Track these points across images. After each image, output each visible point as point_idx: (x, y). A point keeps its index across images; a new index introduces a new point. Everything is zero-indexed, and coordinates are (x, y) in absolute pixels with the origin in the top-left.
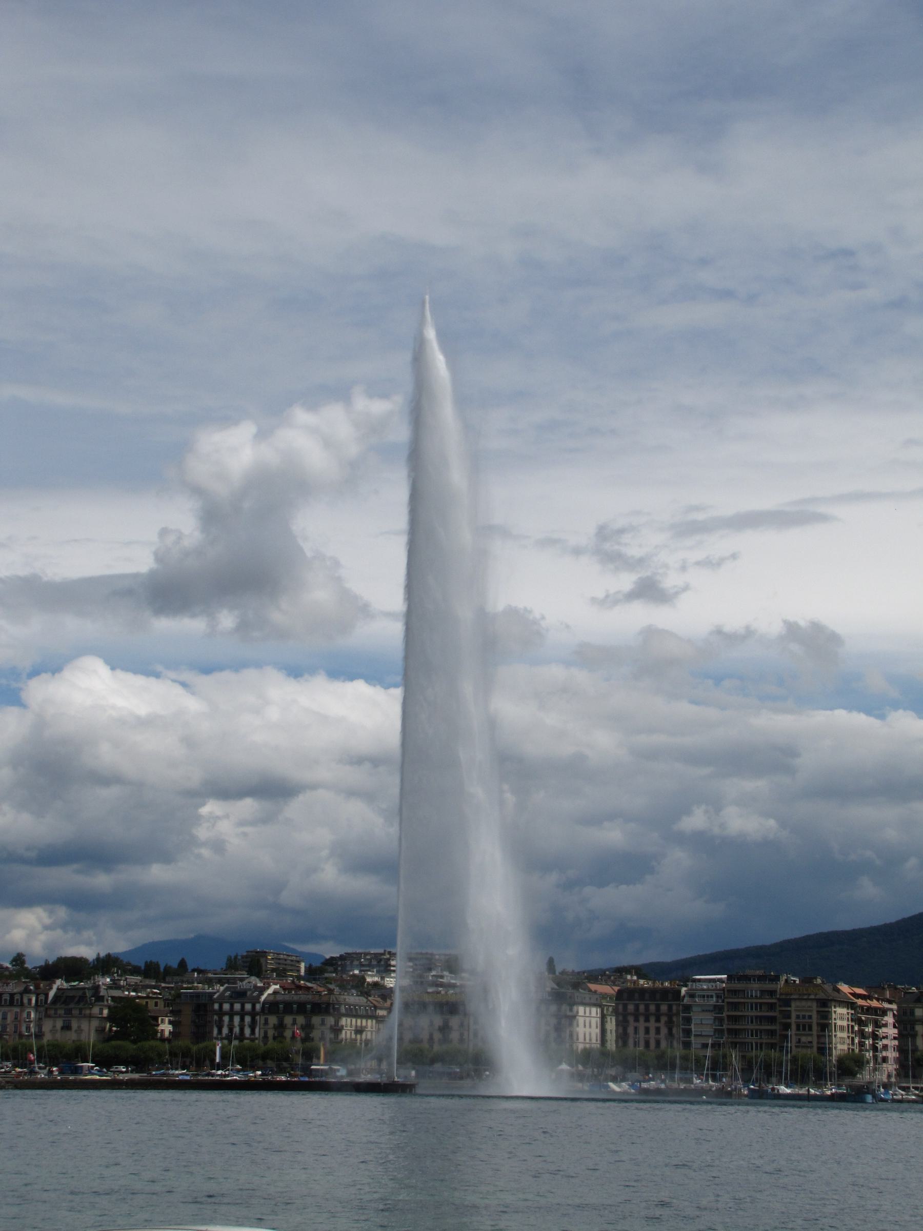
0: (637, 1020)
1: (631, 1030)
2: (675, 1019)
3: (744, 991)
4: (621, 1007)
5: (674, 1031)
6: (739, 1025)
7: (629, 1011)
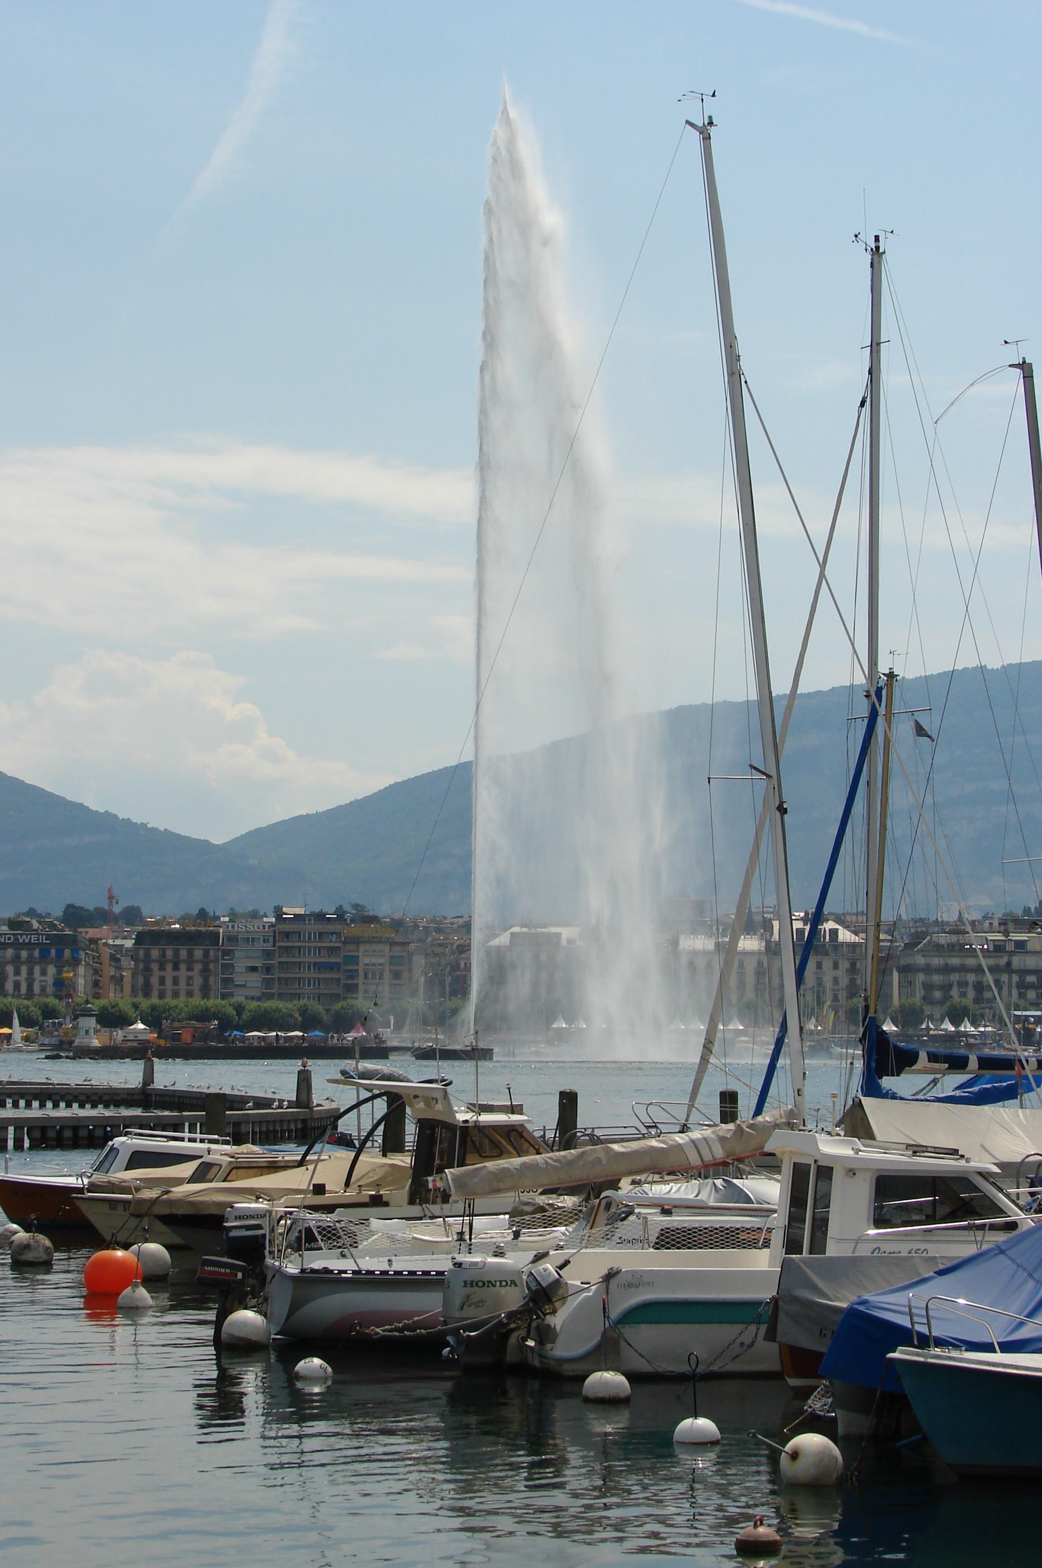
0: (162, 968)
1: (154, 981)
2: (212, 966)
3: (300, 933)
4: (141, 953)
5: (212, 980)
6: (292, 973)
7: (181, 958)
